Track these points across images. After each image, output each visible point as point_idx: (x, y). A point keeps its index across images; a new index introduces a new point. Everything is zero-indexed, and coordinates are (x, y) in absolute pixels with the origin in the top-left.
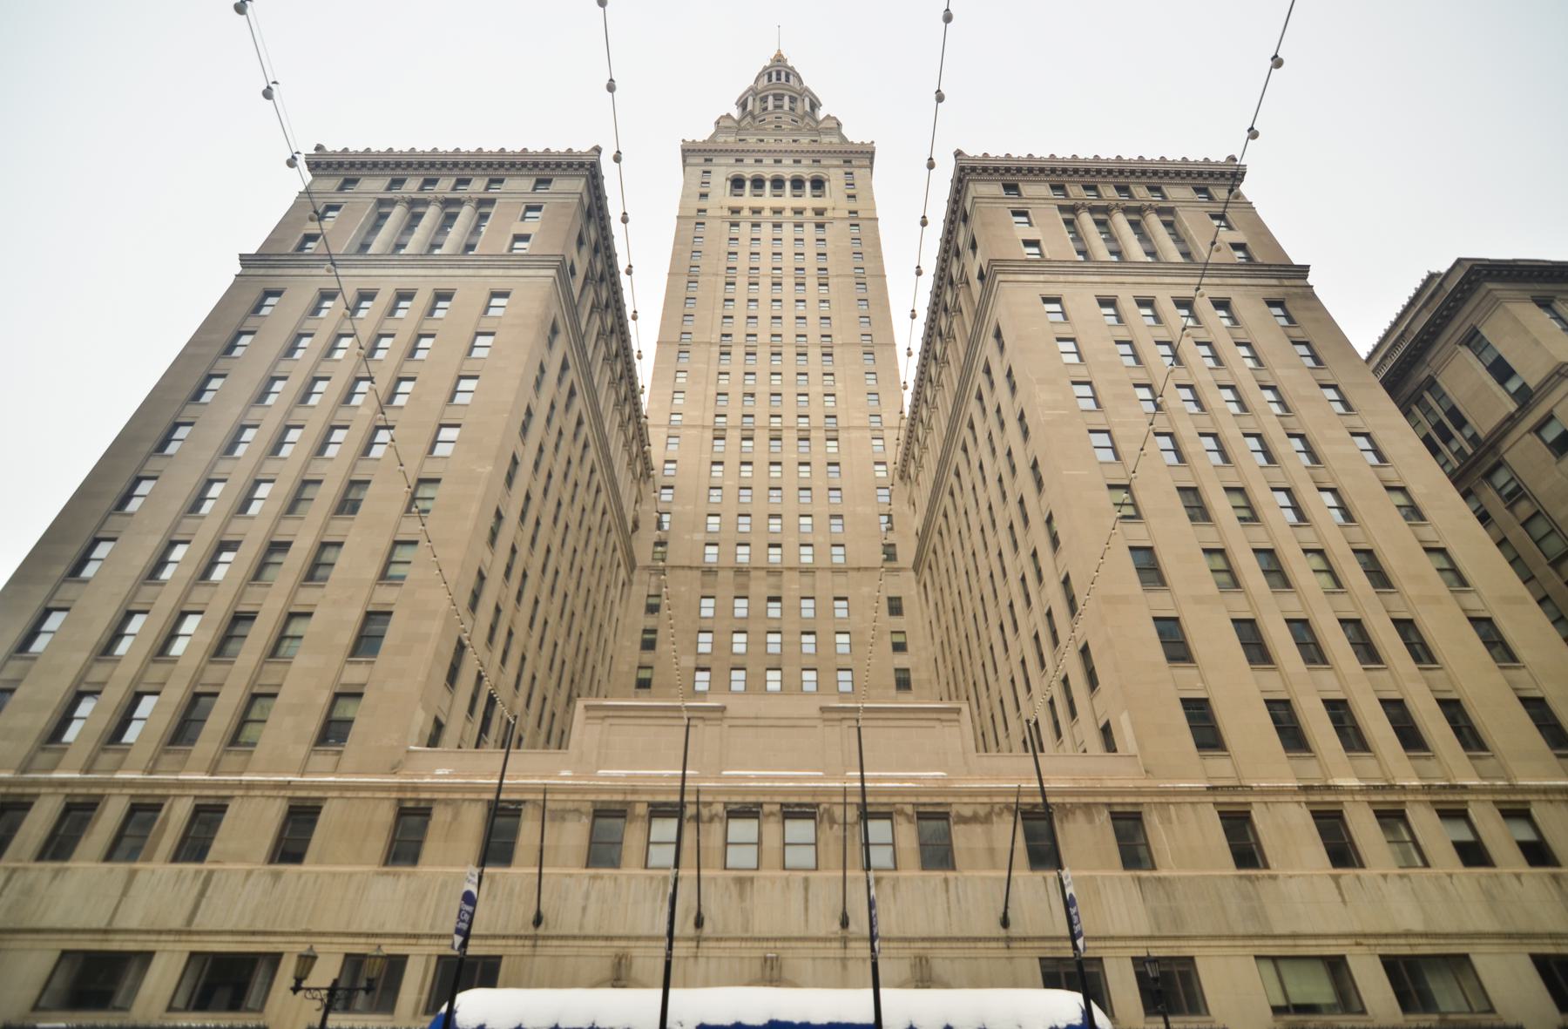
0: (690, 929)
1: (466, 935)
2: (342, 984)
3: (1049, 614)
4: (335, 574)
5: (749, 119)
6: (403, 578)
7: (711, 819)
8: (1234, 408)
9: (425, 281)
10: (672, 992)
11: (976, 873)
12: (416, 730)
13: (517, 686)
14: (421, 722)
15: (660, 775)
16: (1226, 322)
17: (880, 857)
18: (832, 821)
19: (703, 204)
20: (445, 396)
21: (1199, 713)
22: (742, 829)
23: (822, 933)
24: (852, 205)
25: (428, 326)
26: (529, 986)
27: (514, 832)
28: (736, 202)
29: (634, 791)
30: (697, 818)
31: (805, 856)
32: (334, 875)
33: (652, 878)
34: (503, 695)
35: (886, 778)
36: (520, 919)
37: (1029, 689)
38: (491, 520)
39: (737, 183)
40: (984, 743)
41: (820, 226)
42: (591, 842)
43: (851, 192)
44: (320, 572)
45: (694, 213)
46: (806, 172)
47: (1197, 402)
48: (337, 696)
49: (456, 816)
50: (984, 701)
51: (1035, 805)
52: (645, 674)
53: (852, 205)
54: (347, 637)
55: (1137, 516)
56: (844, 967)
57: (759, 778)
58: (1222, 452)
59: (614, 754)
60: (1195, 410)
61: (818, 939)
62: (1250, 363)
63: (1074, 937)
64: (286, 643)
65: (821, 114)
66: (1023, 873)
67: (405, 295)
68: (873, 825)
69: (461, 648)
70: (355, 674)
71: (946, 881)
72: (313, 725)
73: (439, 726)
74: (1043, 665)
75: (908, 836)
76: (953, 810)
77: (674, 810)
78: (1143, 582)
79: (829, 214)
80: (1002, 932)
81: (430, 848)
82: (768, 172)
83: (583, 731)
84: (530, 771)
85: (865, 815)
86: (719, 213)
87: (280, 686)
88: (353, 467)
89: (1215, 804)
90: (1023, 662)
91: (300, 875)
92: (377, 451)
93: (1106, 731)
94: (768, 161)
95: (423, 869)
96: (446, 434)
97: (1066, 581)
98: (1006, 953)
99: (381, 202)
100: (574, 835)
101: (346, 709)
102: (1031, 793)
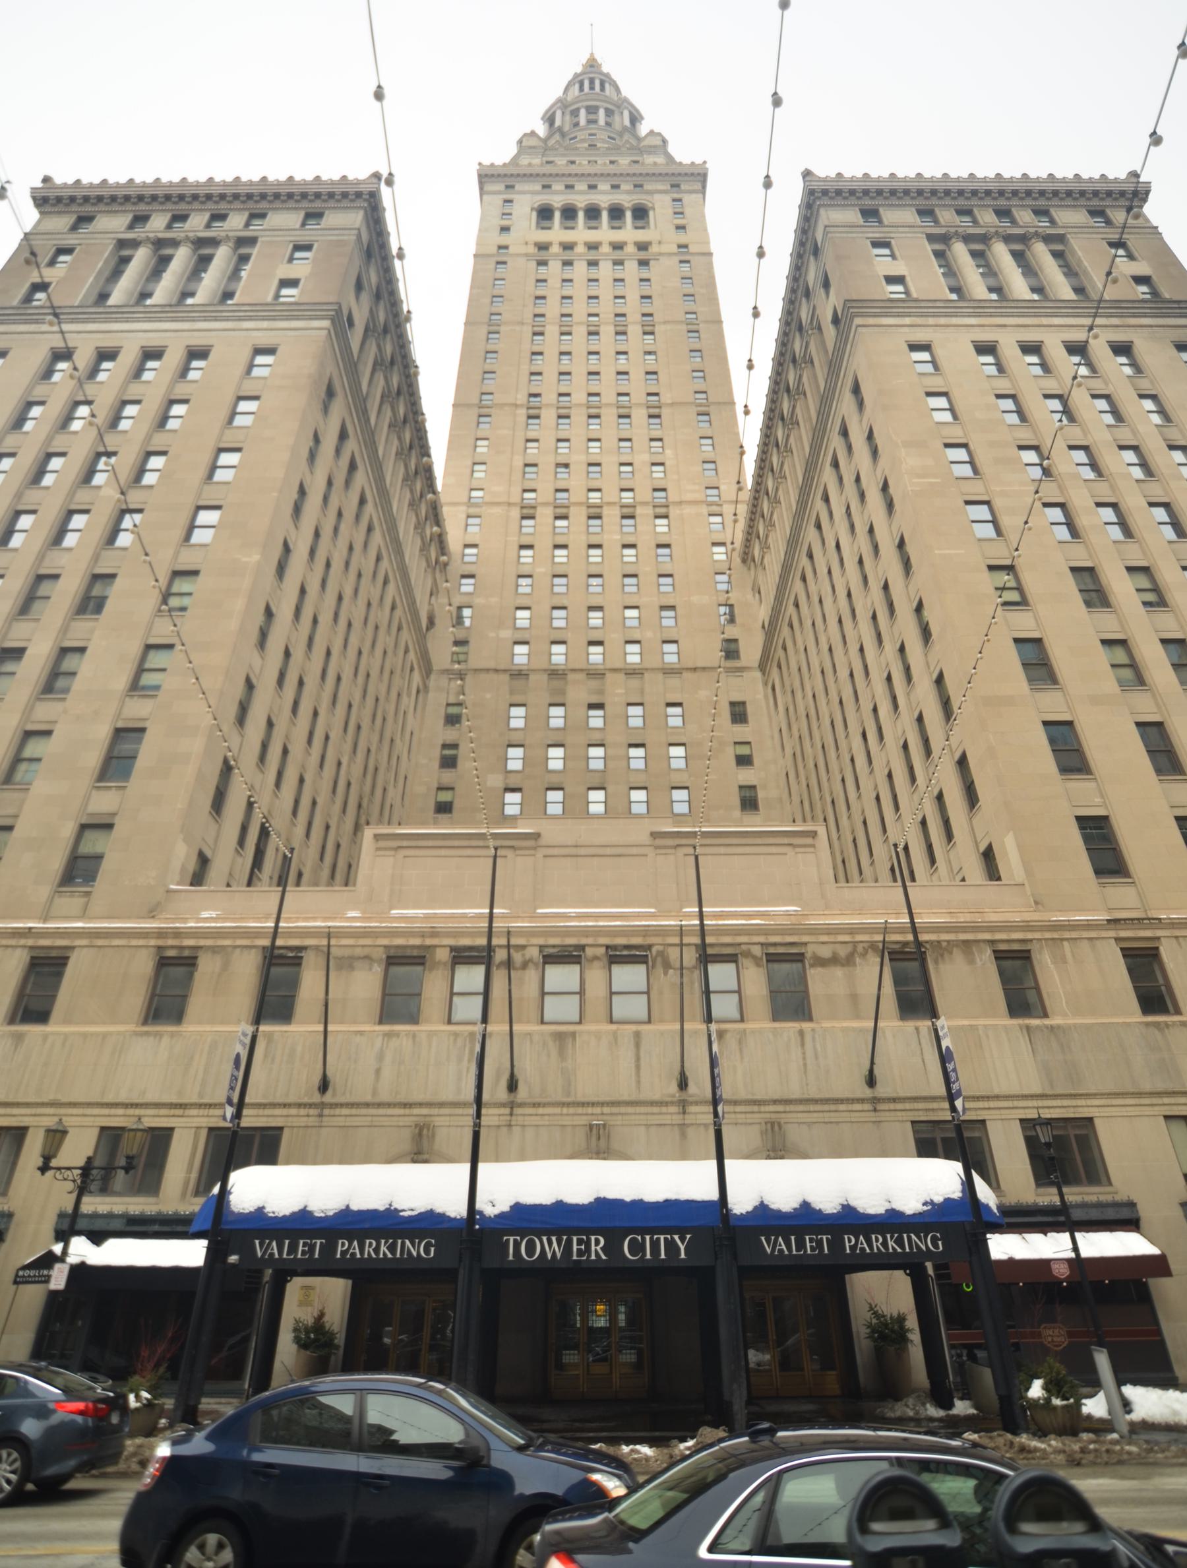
0: (502, 1094)
1: (240, 1106)
2: (97, 1163)
3: (920, 719)
4: (78, 684)
5: (557, 137)
6: (157, 688)
7: (525, 965)
8: (1137, 473)
9: (175, 336)
10: (482, 1167)
11: (837, 1024)
12: (177, 864)
13: (295, 813)
14: (182, 855)
15: (464, 914)
16: (1128, 371)
17: (723, 1006)
18: (667, 966)
19: (504, 239)
20: (202, 472)
21: (1098, 834)
22: (561, 977)
23: (657, 1097)
24: (682, 238)
25: (181, 390)
26: (315, 1163)
27: (294, 984)
28: (543, 236)
29: (434, 934)
30: (509, 964)
31: (635, 1007)
32: (85, 1036)
33: (456, 1035)
34: (278, 824)
35: (730, 914)
36: (303, 1083)
37: (897, 808)
38: (260, 618)
39: (545, 214)
40: (846, 871)
41: (643, 263)
42: (384, 994)
43: (680, 222)
44: (61, 683)
45: (494, 250)
46: (626, 199)
47: (1094, 466)
48: (84, 827)
49: (226, 966)
50: (844, 822)
51: (906, 944)
52: (444, 797)
53: (682, 238)
54: (93, 759)
55: (1023, 602)
56: (683, 1135)
57: (580, 917)
58: (1123, 524)
59: (408, 893)
60: (1091, 475)
61: (652, 1103)
62: (1156, 419)
63: (951, 1097)
64: (23, 767)
65: (643, 129)
66: (891, 1023)
67: (152, 354)
68: (713, 969)
69: (227, 769)
70: (104, 802)
71: (801, 1033)
72: (56, 863)
73: (203, 861)
74: (913, 779)
75: (756, 981)
76: (809, 951)
77: (482, 956)
78: (1030, 680)
79: (654, 249)
80: (868, 1093)
81: (197, 1003)
82: (581, 200)
83: (372, 864)
84: (310, 913)
85: (706, 958)
86: (523, 250)
87: (16, 816)
88: (96, 558)
89: (1117, 939)
90: (890, 776)
91: (45, 1037)
92: (124, 539)
93: (988, 856)
94: (581, 186)
95: (189, 1028)
96: (204, 517)
97: (940, 680)
98: (872, 1116)
99: (122, 244)
100: (364, 985)
101: (93, 843)
102: (900, 930)
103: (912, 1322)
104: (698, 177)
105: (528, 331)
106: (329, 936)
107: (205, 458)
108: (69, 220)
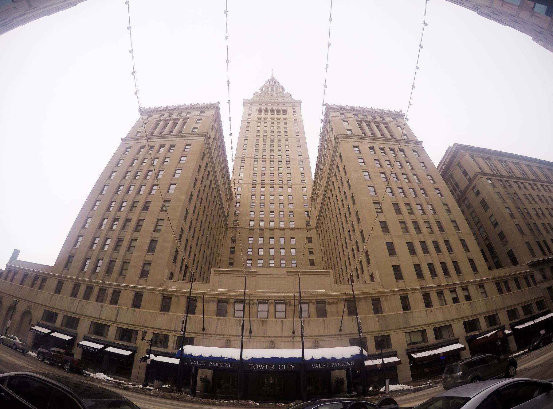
0: (248, 334)
1: (185, 332)
2: (153, 340)
3: (357, 242)
4: (143, 228)
6: (160, 230)
7: (253, 304)
8: (406, 180)
9: (167, 142)
11: (332, 318)
12: (166, 275)
13: (193, 263)
14: (167, 272)
15: (238, 291)
16: (403, 156)
17: (305, 314)
18: (290, 305)
20: (172, 175)
21: (397, 270)
22: (262, 307)
23: (287, 335)
24: (295, 117)
25: (168, 155)
27: (195, 305)
28: (260, 116)
29: (230, 296)
30: (249, 304)
31: (282, 315)
32: (148, 312)
33: (236, 320)
34: (190, 266)
35: (307, 292)
36: (199, 328)
37: (350, 265)
38: (185, 213)
39: (260, 111)
40: (337, 281)
41: (285, 123)
42: (217, 309)
44: (139, 228)
46: (281, 108)
47: (397, 178)
48: (145, 264)
49: (179, 300)
50: (337, 268)
51: (351, 298)
52: (231, 261)
54: (146, 247)
55: (382, 212)
56: (293, 344)
57: (267, 292)
58: (404, 193)
59: (222, 285)
60: (397, 181)
61: (286, 337)
62: (410, 168)
63: (359, 333)
64: (131, 248)
65: (285, 92)
66: (346, 317)
67: (162, 146)
68: (303, 305)
69: (177, 251)
70: (149, 258)
71: (324, 320)
72: (139, 272)
73: (172, 274)
74: (354, 257)
75: (313, 309)
76: (327, 301)
77: (243, 301)
78: (383, 232)
79: (288, 120)
80: (339, 333)
81: (172, 308)
83: (214, 278)
84: (198, 288)
85: (301, 303)
86: (254, 119)
88: (147, 197)
90: (349, 257)
91: (140, 311)
92: (153, 192)
93: (372, 276)
94: (269, 105)
95: (171, 313)
96: (172, 187)
97: (362, 232)
98: (340, 338)
99: (158, 121)
100: (213, 307)
101: (147, 268)
102: (350, 295)
103: (345, 379)
104: (299, 103)
105: (255, 139)
106: (203, 295)
107: (173, 172)
108: (147, 116)
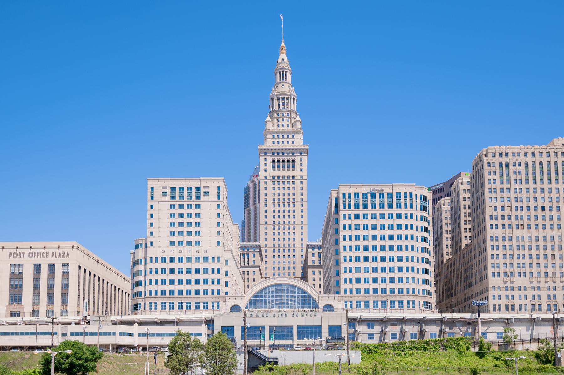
39: (273, 161)
79: (296, 178)
